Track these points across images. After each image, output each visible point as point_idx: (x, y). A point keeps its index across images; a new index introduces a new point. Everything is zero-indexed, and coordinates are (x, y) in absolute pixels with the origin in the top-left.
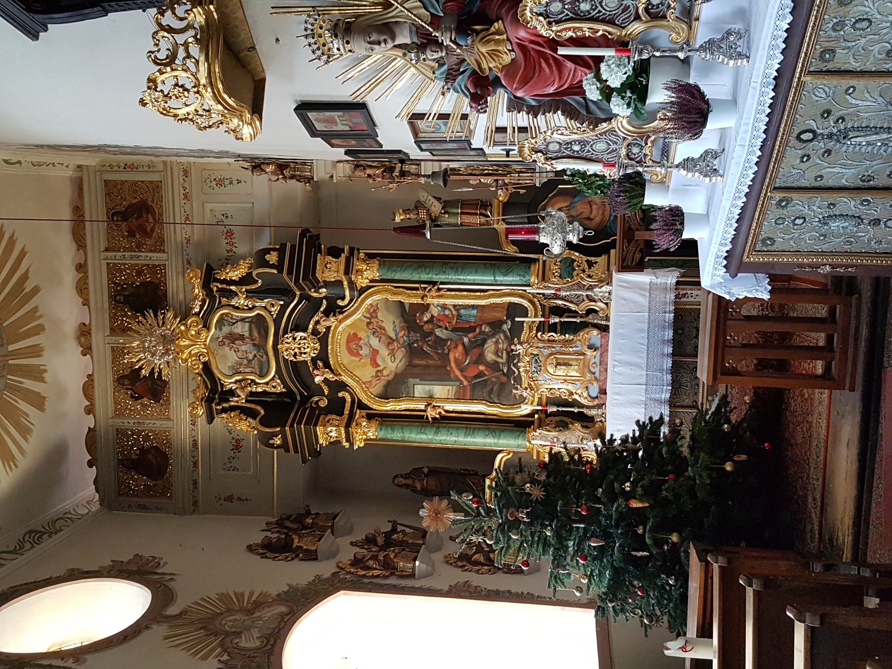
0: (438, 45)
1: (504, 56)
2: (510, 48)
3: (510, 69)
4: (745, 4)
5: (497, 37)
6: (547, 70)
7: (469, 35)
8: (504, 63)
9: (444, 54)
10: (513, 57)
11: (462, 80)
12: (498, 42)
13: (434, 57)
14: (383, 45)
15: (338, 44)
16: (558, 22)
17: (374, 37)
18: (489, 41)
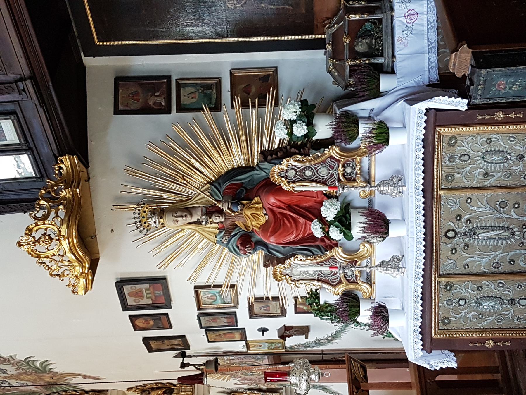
0: (220, 212)
1: (261, 218)
2: (265, 212)
3: (264, 228)
4: (399, 168)
5: (257, 205)
6: (288, 225)
7: (239, 205)
8: (261, 223)
9: (223, 220)
10: (267, 219)
11: (234, 241)
12: (257, 209)
13: (217, 221)
14: (184, 218)
15: (155, 219)
16: (294, 182)
17: (179, 214)
18: (252, 208)
